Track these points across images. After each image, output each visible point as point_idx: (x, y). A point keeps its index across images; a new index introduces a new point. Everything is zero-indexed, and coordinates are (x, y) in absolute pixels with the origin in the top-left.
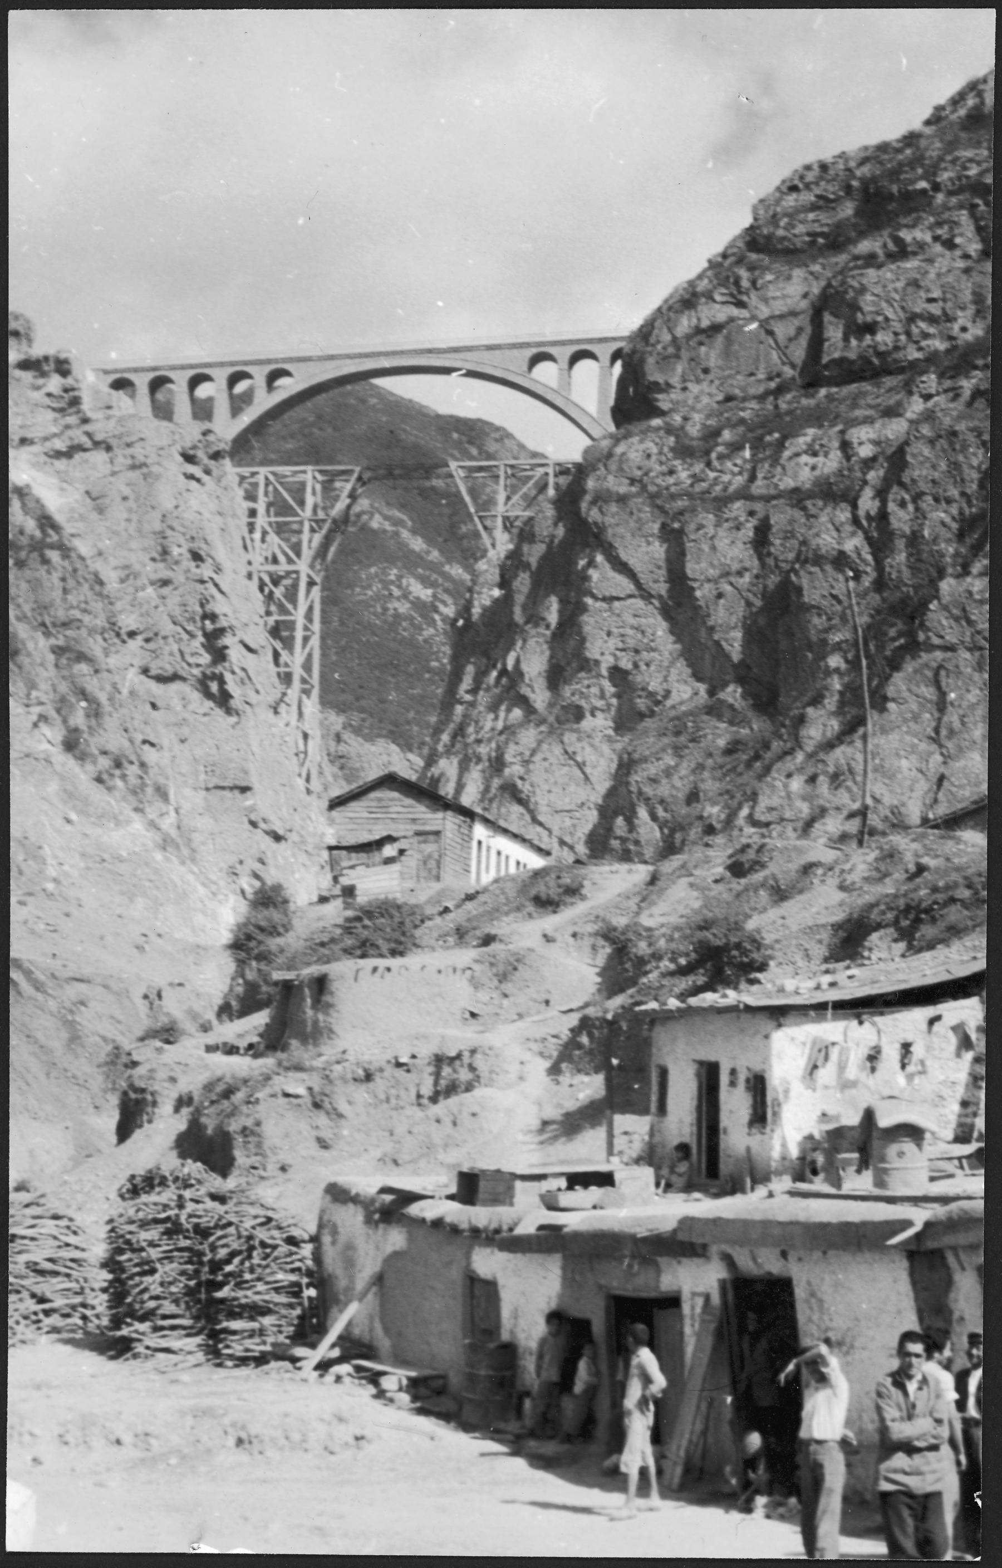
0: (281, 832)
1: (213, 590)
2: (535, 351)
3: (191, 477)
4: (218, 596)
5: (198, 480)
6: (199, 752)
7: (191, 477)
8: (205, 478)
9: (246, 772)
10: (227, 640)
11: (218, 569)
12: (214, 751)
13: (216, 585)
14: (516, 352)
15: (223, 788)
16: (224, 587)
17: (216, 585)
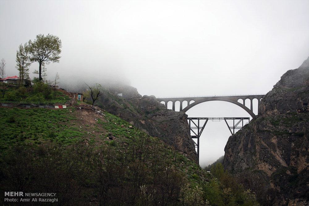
16: (190, 143)
17: (189, 142)
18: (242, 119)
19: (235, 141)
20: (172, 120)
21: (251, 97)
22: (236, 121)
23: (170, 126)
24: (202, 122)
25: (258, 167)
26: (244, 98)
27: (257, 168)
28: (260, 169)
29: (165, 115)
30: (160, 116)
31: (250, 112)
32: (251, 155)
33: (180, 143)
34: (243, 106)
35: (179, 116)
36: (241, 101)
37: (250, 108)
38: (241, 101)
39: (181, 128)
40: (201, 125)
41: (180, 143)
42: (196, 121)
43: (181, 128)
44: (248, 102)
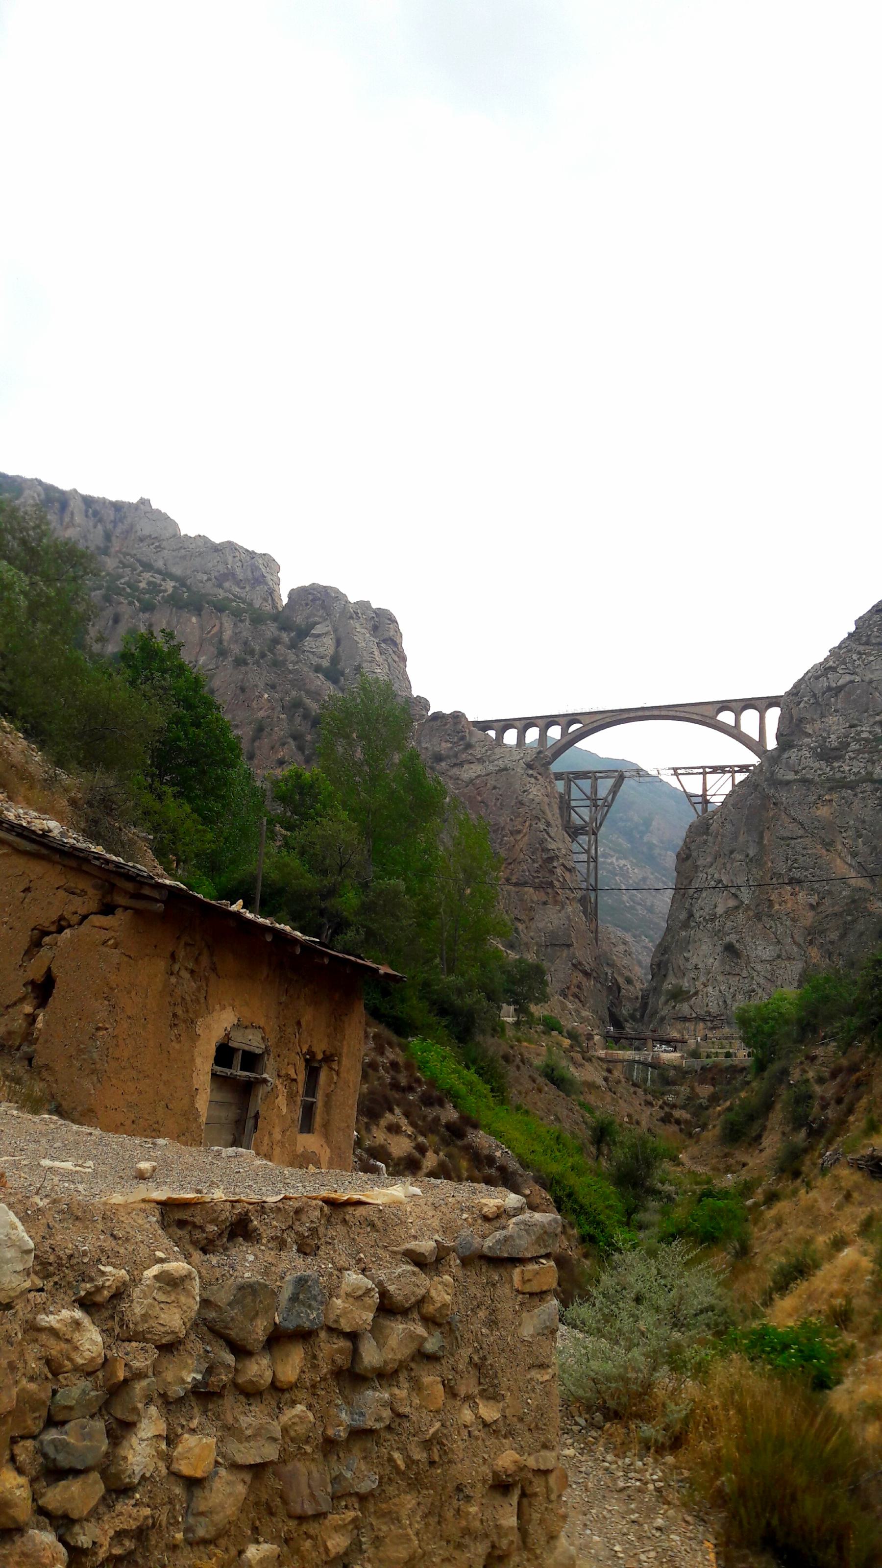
0: (589, 971)
1: (546, 836)
2: (721, 705)
3: (531, 776)
4: (549, 839)
5: (536, 778)
6: (541, 925)
7: (531, 776)
8: (539, 777)
9: (569, 936)
10: (555, 864)
11: (548, 824)
12: (549, 925)
13: (548, 834)
14: (709, 707)
15: (555, 945)
16: (552, 835)
17: (548, 834)
18: (730, 770)
19: (707, 834)
20: (502, 770)
21: (762, 704)
22: (711, 778)
23: (495, 788)
24: (605, 787)
25: (769, 900)
26: (740, 706)
27: (767, 903)
28: (777, 907)
29: (484, 761)
30: (472, 766)
31: (757, 747)
32: (747, 863)
33: (522, 835)
34: (734, 732)
35: (522, 758)
36: (727, 717)
37: (756, 736)
38: (727, 717)
39: (524, 791)
40: (603, 792)
41: (522, 835)
42: (586, 784)
43: (524, 791)
44: (749, 721)
